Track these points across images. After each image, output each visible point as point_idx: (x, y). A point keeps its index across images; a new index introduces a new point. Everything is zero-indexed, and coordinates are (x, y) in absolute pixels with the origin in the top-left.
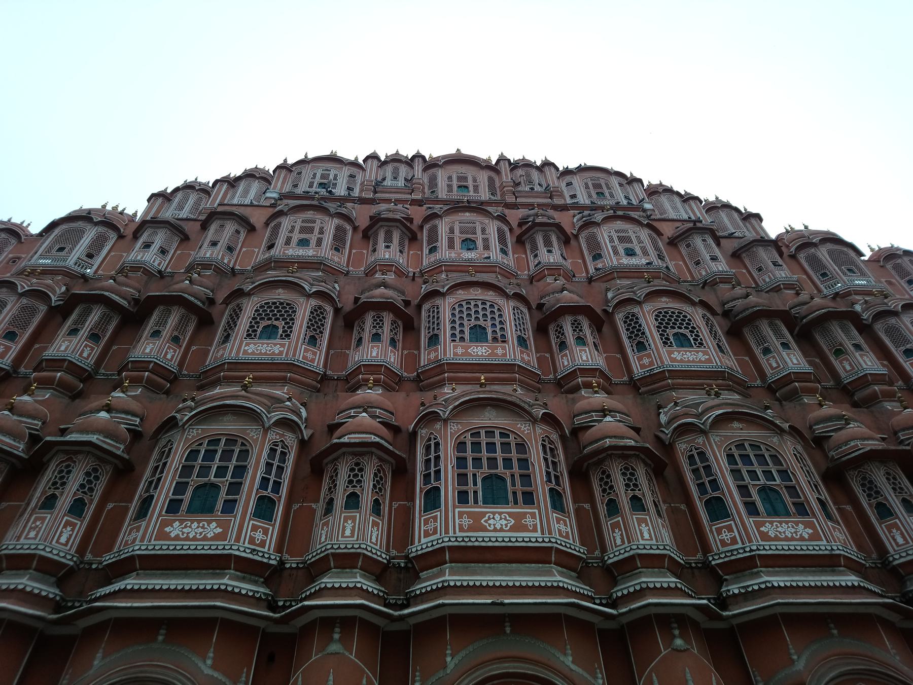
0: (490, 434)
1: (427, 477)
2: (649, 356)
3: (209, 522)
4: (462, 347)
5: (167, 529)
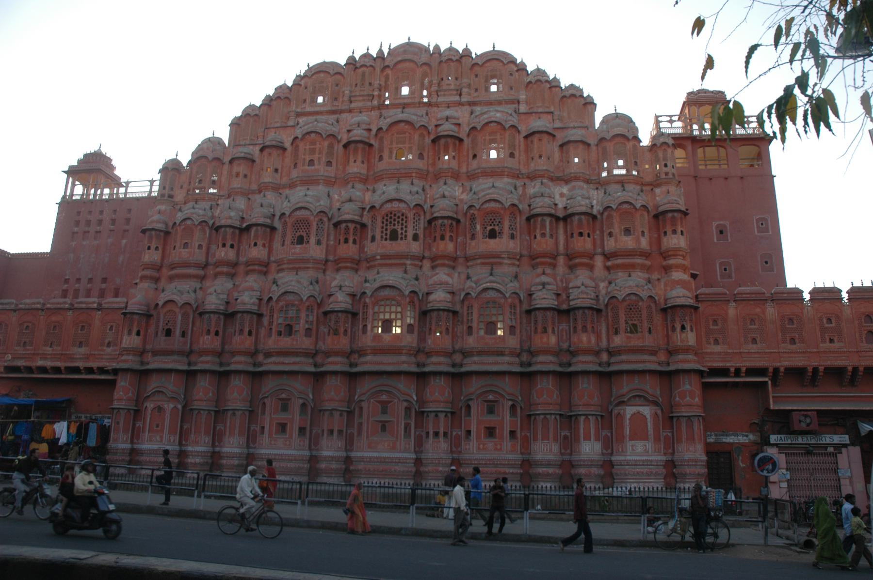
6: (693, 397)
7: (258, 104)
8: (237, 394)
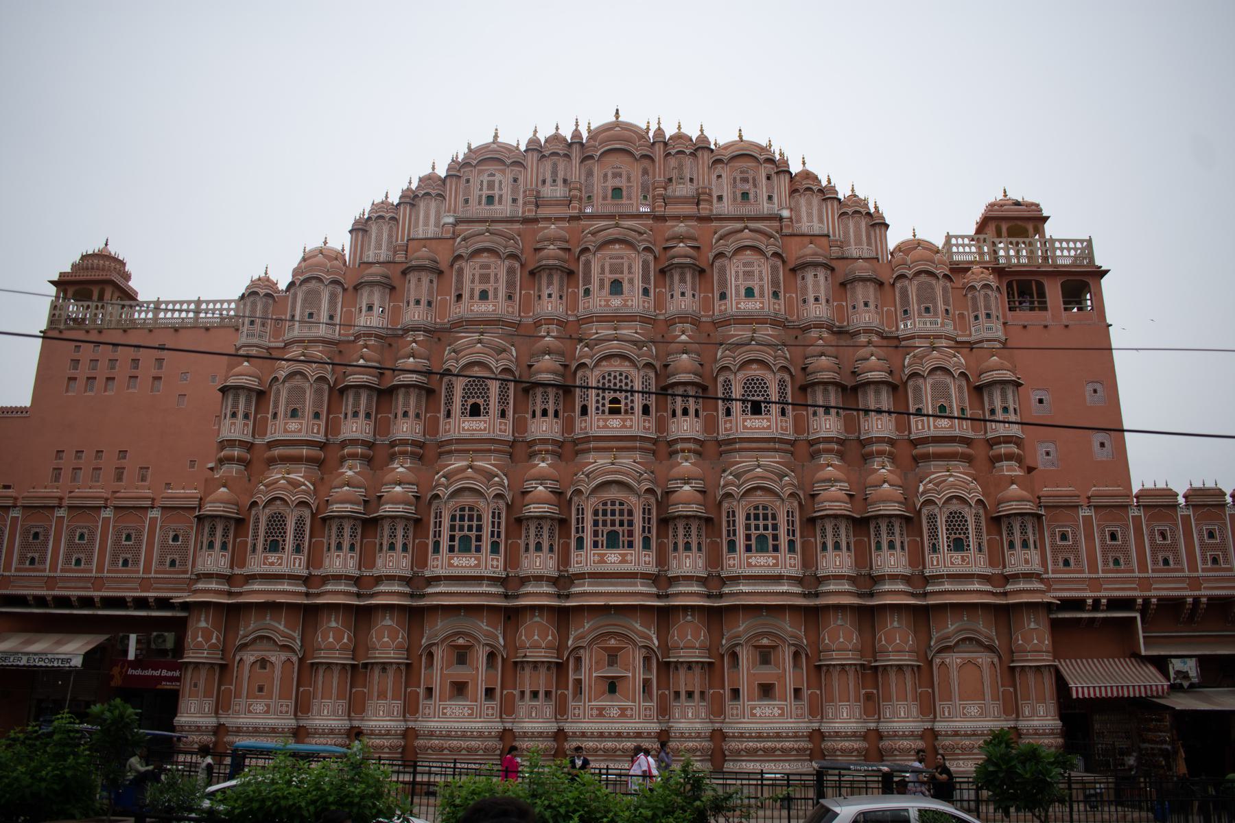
0: (613, 503)
1: (577, 529)
6: (1041, 641)
7: (394, 199)
8: (386, 642)
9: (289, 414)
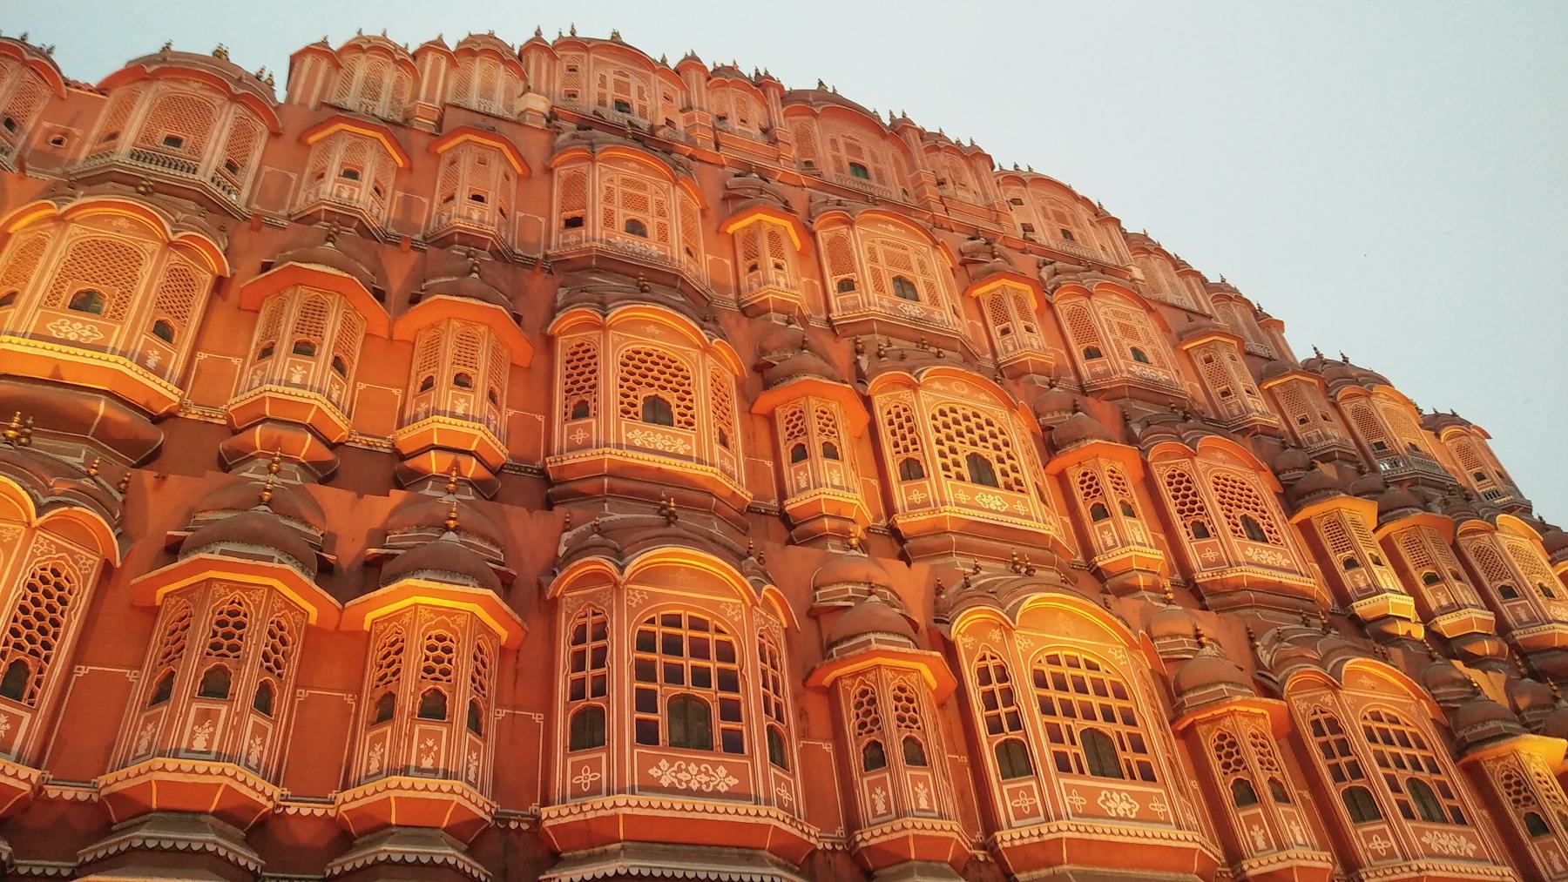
2: (1214, 547)
3: (715, 765)
4: (967, 491)
5: (653, 772)
9: (67, 297)
